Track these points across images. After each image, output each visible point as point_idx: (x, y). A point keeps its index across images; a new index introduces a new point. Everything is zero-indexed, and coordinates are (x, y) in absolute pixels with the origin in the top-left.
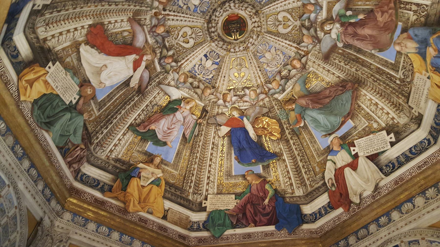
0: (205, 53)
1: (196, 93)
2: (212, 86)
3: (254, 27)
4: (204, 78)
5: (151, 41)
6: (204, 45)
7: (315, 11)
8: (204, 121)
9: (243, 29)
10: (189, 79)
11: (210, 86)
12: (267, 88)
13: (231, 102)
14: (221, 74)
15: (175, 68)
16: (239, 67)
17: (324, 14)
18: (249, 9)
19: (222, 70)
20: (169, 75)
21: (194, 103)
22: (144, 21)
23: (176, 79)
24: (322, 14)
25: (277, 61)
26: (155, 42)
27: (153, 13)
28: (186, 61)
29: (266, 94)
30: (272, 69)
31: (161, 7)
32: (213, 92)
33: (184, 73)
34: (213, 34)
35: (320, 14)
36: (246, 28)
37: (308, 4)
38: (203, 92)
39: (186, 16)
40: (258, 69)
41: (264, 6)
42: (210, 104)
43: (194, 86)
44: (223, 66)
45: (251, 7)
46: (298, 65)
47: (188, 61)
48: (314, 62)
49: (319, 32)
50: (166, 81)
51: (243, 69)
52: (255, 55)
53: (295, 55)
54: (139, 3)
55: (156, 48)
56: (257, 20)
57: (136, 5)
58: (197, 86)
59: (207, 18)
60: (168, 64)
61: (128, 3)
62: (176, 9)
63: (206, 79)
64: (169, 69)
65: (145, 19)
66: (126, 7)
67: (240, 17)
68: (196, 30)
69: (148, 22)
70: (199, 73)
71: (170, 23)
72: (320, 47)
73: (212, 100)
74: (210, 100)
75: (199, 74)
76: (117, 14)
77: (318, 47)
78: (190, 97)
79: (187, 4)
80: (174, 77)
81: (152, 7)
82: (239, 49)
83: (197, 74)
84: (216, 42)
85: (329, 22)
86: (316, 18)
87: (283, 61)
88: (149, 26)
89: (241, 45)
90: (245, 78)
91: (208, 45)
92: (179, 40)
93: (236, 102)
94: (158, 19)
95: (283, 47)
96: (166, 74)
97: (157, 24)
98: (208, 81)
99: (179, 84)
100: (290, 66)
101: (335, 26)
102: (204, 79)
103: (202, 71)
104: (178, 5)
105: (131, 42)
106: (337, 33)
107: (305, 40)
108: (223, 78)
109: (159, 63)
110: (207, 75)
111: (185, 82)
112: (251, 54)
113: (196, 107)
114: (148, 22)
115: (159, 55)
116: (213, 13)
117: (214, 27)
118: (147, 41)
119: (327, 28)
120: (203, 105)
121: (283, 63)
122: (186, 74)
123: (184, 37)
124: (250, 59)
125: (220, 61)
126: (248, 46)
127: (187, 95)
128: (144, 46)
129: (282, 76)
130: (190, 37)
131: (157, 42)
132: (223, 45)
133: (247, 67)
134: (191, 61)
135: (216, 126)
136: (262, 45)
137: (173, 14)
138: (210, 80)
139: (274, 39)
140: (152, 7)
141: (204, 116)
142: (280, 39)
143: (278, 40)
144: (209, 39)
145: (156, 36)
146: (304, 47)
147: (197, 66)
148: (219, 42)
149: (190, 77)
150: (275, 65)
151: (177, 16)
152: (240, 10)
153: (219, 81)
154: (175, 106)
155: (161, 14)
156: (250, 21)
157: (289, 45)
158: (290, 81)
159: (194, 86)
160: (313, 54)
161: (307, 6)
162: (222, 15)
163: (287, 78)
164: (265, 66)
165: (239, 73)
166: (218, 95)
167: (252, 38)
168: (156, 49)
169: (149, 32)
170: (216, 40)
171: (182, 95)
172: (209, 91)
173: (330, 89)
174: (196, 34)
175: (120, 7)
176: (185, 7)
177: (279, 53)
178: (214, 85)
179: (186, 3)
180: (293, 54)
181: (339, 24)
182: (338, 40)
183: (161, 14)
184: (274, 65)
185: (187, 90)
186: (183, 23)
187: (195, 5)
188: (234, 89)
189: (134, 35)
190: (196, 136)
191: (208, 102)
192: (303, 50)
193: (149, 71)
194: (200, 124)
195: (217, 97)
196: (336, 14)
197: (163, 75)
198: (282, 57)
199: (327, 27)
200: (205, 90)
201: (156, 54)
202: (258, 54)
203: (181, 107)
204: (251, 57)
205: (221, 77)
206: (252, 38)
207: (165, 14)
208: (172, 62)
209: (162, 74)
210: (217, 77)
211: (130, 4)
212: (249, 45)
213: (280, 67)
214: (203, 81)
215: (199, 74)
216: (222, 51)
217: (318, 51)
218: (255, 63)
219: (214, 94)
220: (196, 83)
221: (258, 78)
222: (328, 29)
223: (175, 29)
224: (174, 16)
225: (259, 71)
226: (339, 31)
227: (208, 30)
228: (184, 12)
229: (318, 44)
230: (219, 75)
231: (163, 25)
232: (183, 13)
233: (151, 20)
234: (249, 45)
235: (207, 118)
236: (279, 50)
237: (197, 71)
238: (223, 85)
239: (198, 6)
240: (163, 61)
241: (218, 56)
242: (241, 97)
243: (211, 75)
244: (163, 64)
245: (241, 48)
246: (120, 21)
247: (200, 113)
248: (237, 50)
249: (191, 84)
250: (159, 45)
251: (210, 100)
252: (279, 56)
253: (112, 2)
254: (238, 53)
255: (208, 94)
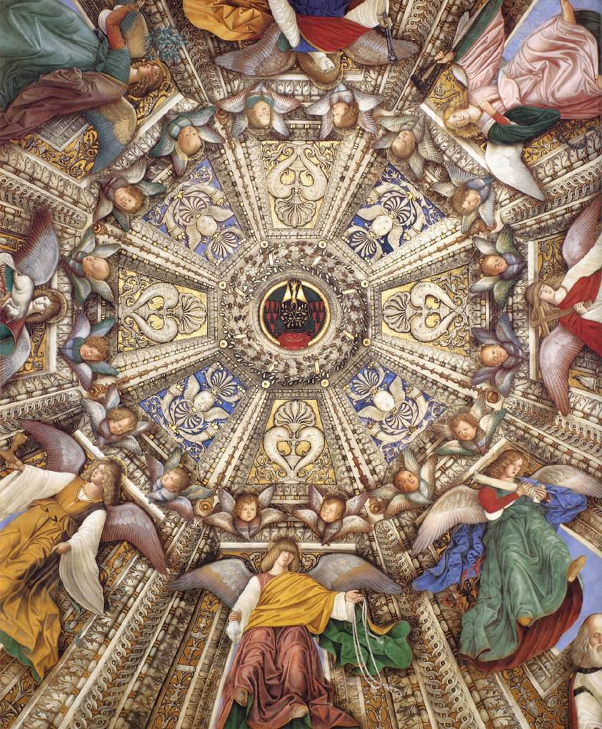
0: (389, 258)
1: (436, 147)
2: (385, 157)
3: (241, 307)
4: (406, 188)
5: (529, 336)
6: (386, 278)
7: (78, 343)
8: (429, 54)
9: (273, 306)
10: (449, 195)
11: (389, 158)
12: (215, 131)
13: (334, 100)
14: (353, 189)
15: (482, 235)
16: (297, 201)
17: (53, 339)
18: (251, 353)
19: (348, 198)
20: (506, 220)
21: (452, 120)
22: (529, 391)
23: (489, 205)
24: (58, 335)
25: (182, 208)
26: (518, 327)
27: (500, 403)
28: (446, 247)
29: (221, 110)
30: (201, 186)
31: (476, 411)
32: (385, 140)
33: (460, 215)
34: (357, 303)
35: (65, 338)
36: (265, 308)
37: (97, 361)
38: (416, 145)
39: (418, 369)
40: (240, 188)
41: (213, 359)
42: (400, 104)
43: (438, 172)
44: (342, 210)
45: (245, 358)
46: (121, 196)
47: (441, 244)
48: (76, 203)
49: (66, 288)
50: (521, 205)
51: (285, 192)
52: (247, 229)
53: (133, 224)
54: (529, 442)
55: (519, 311)
56: (233, 324)
57: (537, 441)
58: (430, 168)
59: (362, 351)
60: (501, 255)
61: (557, 452)
62: (438, 394)
63: (399, 184)
64: (500, 237)
65: (525, 394)
66: (565, 446)
67: (277, 338)
68: (398, 324)
69: (521, 386)
70: (416, 204)
71: (465, 363)
72: (61, 245)
73: (391, 114)
74: (397, 116)
75: (418, 201)
76: (592, 437)
77: (67, 247)
78: (459, 142)
79: (407, 399)
80: (495, 209)
81: (500, 417)
82: (291, 252)
83: (424, 203)
84: (350, 279)
85: (37, 318)
86: (74, 327)
87: (165, 209)
88: (522, 375)
89: (283, 261)
90: (282, 166)
91: (375, 277)
92: (452, 310)
93: (318, 98)
94: (492, 382)
95: (165, 244)
96: (516, 226)
97: (499, 372)
98: (394, 176)
99: (484, 187)
100: (146, 194)
101: (23, 308)
102: (404, 184)
103: (408, 208)
104: (431, 404)
105: (581, 354)
106: (14, 290)
107: (103, 265)
108: (349, 174)
109: (526, 266)
110: (395, 194)
111: (465, 188)
112: (257, 234)
113: (448, 107)
114: (521, 386)
115: (519, 290)
116: (345, 361)
117: (349, 320)
118: (540, 340)
119: (43, 303)
120: (423, 107)
121: (167, 202)
122: (455, 210)
123: (439, 314)
124: (263, 218)
125: (350, 226)
126: (262, 257)
127: (466, 147)
128: (551, 330)
129: (171, 166)
130: (419, 311)
131: (513, 328)
132: (331, 270)
133: (271, 197)
134: (433, 241)
135: (393, 28)
136: (225, 255)
137: (450, 384)
138: (387, 176)
139: (189, 270)
140: (500, 417)
141: (428, 68)
142: (173, 267)
143: (178, 265)
144: (369, 294)
145: (511, 343)
146: (106, 245)
147: (418, 226)
148: (342, 277)
149: (445, 198)
150: (188, 198)
151: (441, 375)
152: (275, 353)
153: (362, 170)
154: (513, 127)
155: (481, 392)
156: (251, 322)
157: (149, 252)
158: (146, 151)
159: (438, 172)
160: (82, 224)
161: (98, 357)
162: (325, 349)
163: (154, 158)
164: (219, 196)
165: (297, 183)
166: (370, 128)
167: (249, 278)
168: (521, 307)
169: (526, 360)
170: (349, 286)
171: (484, 153)
172: (398, 144)
173: (22, 128)
174: (402, 315)
175: (579, 453)
176: (415, 392)
177: (178, 232)
178: (379, 159)
179: (410, 402)
180: (138, 225)
181: (12, 317)
182: (13, 271)
183: (481, 392)
184: (192, 199)
185: (462, 163)
186: (428, 351)
187: (388, 390)
188: (319, 139)
189: (570, 366)
190: (469, 11)
191: (407, 112)
192: (109, 236)
193: (561, 253)
194: (446, 46)
195: (375, 119)
196: (21, 343)
197: (523, 227)
198: (169, 219)
199: (45, 305)
200: (408, 151)
201: (525, 296)
202: (237, 231)
203: (494, 117)
204: (257, 224)
205: (352, 180)
206: (249, 278)
207: (470, 388)
208: (486, 257)
209: (528, 229)
210: (366, 180)
211: (552, 449)
212: (259, 259)
213: (177, 192)
214: (408, 178)
215: (418, 201)
216: (339, 254)
217: (66, 235)
218: (247, 208)
219: (381, 132)
220: (432, 177)
221: (243, 162)
222: (41, 299)
223: (455, 342)
224: (447, 378)
225: (239, 182)
226: (11, 296)
227: (367, 317)
228: (419, 379)
229: (66, 254)
230: (360, 186)
231: (484, 363)
232: (424, 378)
233: (512, 387)
234: (259, 259)
235: (420, 62)
236: (178, 240)
237: (419, 210)
238: (351, 157)
239: (381, 386)
240: (511, 268)
241: (351, 241)
242: (299, 111)
243: (381, 189)
244: (514, 259)
245: (283, 252)
246: (591, 418)
247: (438, 84)
248: (297, 249)
249: (446, 179)
250: (510, 315)
251: (397, 116)
252: (178, 223)
253: (594, 476)
254: (294, 239)
255: (400, 135)
